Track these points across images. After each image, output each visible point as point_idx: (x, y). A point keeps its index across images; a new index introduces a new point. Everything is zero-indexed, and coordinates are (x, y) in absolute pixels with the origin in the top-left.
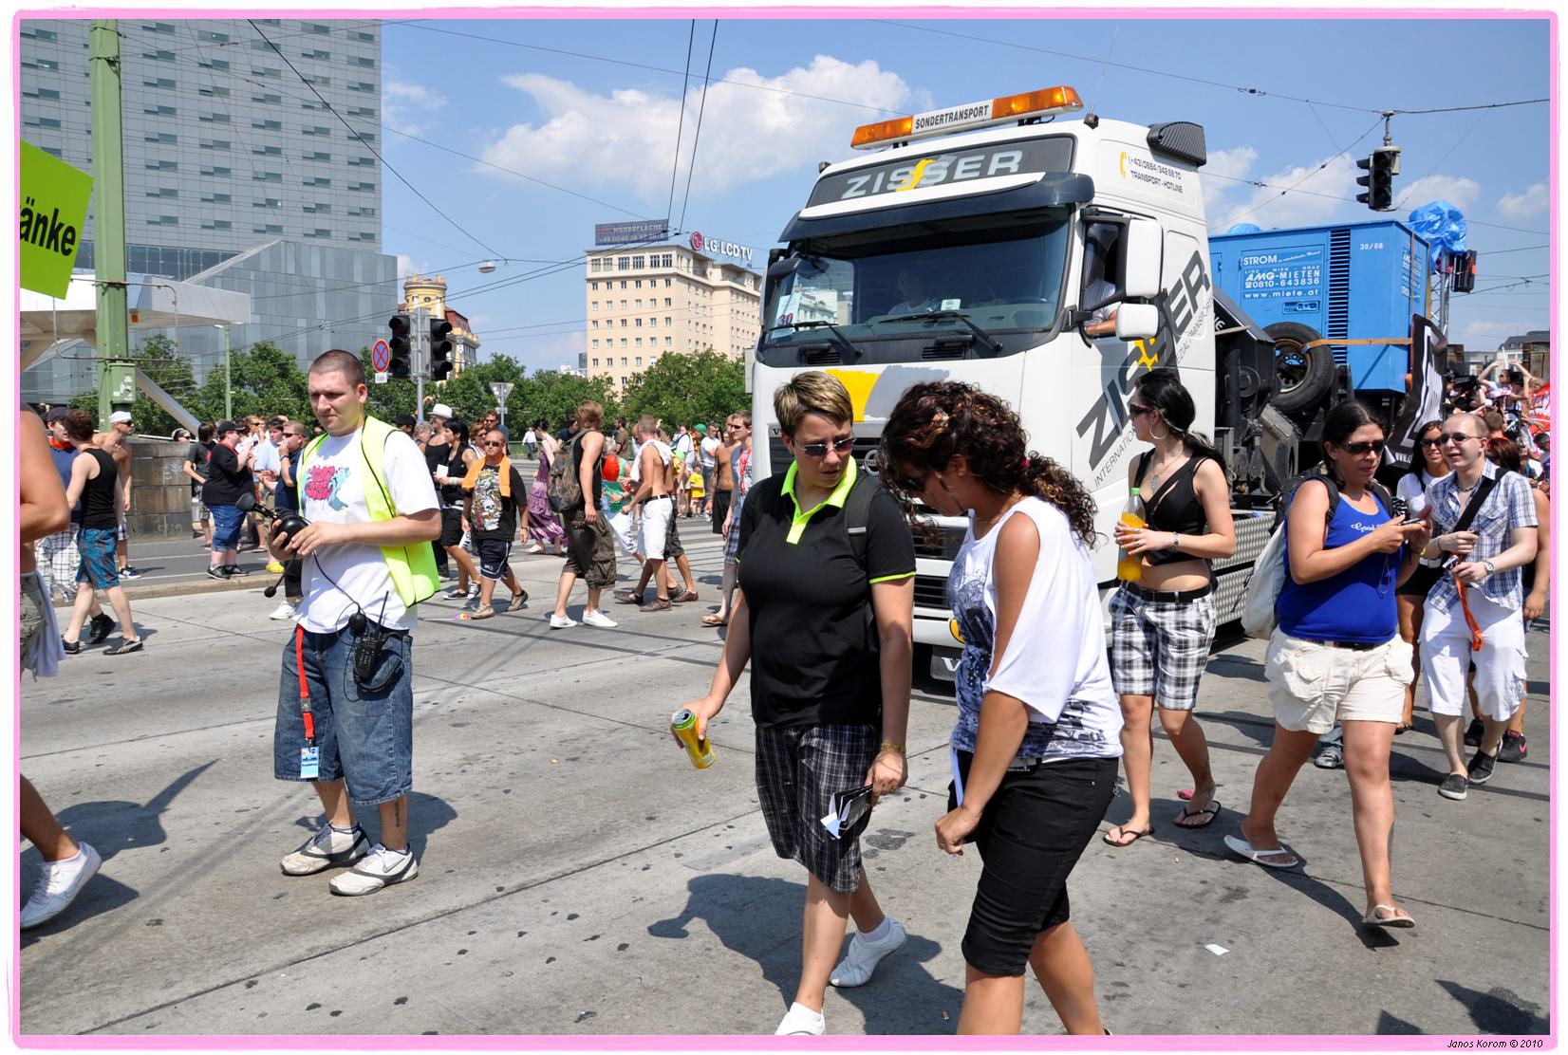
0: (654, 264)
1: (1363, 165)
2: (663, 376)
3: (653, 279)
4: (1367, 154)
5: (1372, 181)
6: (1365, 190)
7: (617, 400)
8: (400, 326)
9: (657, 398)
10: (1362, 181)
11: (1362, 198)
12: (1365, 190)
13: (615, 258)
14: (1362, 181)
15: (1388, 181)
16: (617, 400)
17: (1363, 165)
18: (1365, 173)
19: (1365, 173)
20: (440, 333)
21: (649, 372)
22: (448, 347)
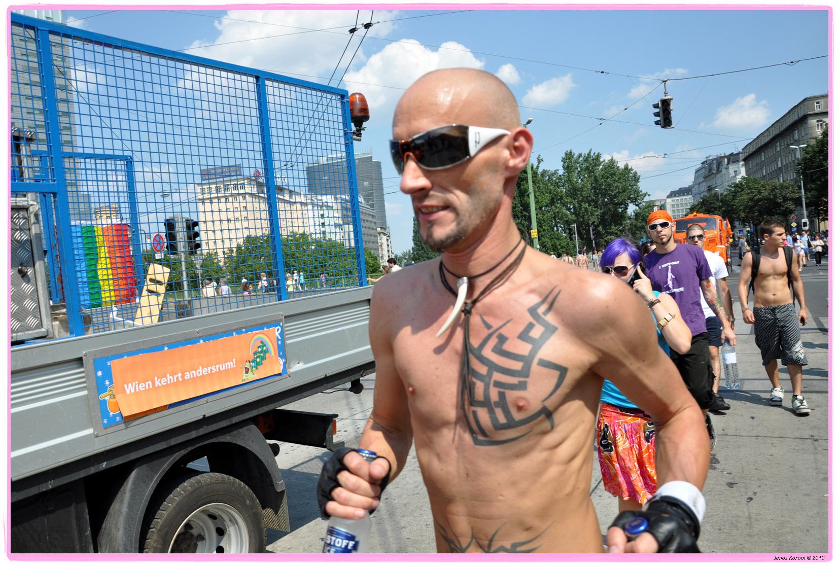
0: (236, 187)
1: (656, 106)
2: (247, 248)
3: (234, 196)
4: (657, 101)
5: (661, 114)
6: (658, 119)
7: (221, 264)
8: (170, 225)
9: (244, 261)
10: (657, 115)
11: (657, 123)
12: (658, 119)
13: (213, 187)
14: (657, 115)
15: (669, 113)
16: (221, 264)
17: (656, 106)
18: (657, 110)
19: (657, 110)
20: (192, 225)
21: (239, 247)
22: (197, 234)
